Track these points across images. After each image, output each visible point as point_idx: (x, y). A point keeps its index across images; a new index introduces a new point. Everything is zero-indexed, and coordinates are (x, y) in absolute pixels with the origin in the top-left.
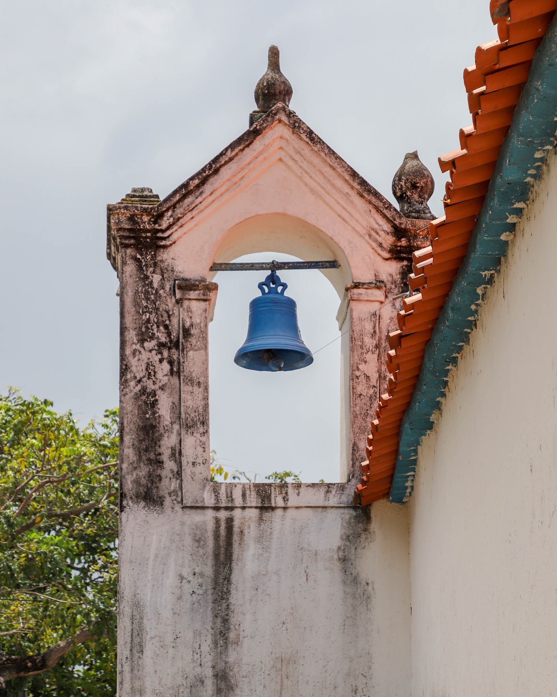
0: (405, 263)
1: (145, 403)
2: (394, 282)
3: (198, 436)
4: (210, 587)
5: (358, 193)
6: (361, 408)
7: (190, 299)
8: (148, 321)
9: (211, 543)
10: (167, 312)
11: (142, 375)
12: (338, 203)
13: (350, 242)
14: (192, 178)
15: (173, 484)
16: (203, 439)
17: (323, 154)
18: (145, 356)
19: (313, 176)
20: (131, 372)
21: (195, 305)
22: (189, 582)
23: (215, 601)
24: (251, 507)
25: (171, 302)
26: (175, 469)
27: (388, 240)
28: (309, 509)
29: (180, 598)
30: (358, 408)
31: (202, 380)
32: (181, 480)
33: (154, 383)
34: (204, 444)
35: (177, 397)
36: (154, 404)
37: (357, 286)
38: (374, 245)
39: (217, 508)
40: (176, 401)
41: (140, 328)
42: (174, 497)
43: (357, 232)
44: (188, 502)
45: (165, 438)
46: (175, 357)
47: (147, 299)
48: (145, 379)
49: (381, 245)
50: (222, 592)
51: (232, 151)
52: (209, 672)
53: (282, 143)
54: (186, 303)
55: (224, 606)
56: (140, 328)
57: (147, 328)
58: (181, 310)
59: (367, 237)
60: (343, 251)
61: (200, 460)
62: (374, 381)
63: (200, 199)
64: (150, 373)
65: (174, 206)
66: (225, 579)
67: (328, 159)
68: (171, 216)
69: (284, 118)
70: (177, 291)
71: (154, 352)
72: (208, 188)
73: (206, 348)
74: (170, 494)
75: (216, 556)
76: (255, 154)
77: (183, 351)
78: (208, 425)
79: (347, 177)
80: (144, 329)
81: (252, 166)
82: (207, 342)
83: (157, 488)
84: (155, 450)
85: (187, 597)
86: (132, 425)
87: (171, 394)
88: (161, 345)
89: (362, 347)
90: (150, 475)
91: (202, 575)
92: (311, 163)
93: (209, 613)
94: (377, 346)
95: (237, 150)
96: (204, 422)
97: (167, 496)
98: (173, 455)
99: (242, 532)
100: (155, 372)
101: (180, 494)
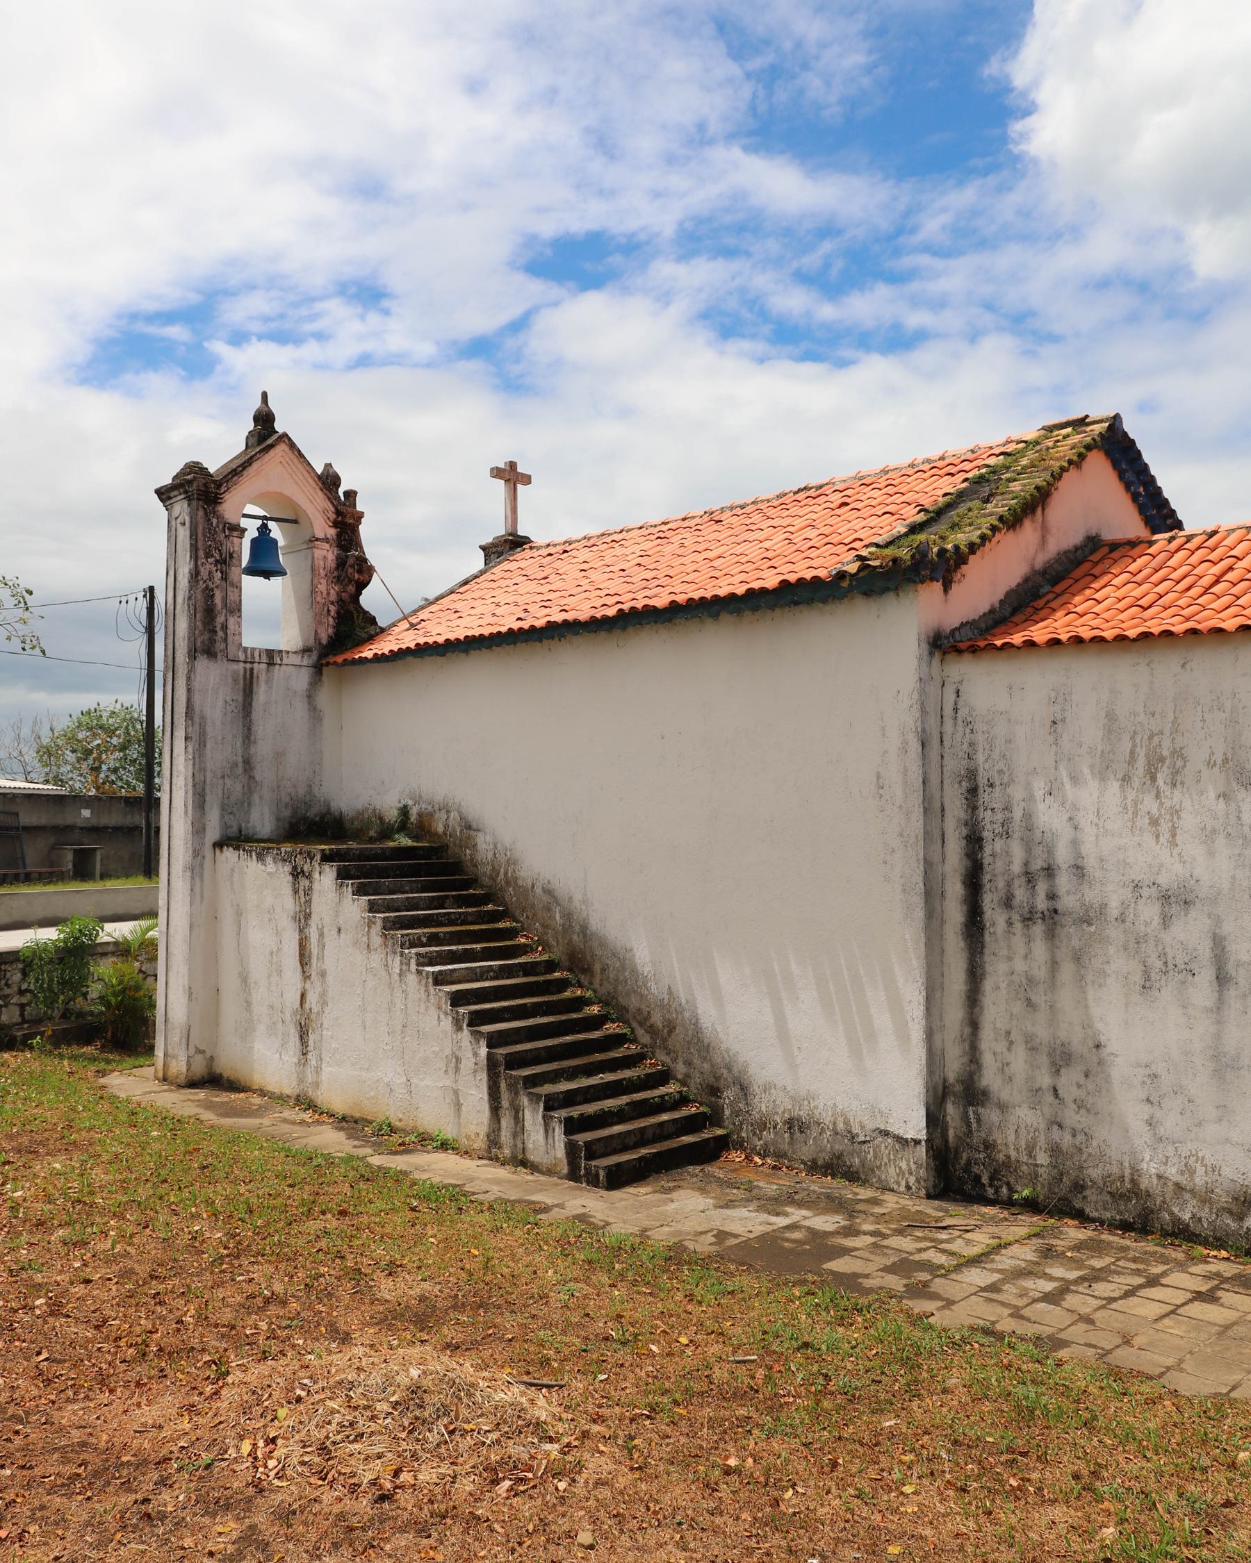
9: (242, 682)
18: (208, 566)
21: (235, 540)
26: (223, 636)
36: (213, 596)
39: (245, 662)
44: (231, 657)
52: (240, 759)
75: (244, 690)
87: (221, 591)
88: (217, 561)
90: (210, 639)
91: (237, 701)
96: (240, 610)
98: (222, 627)
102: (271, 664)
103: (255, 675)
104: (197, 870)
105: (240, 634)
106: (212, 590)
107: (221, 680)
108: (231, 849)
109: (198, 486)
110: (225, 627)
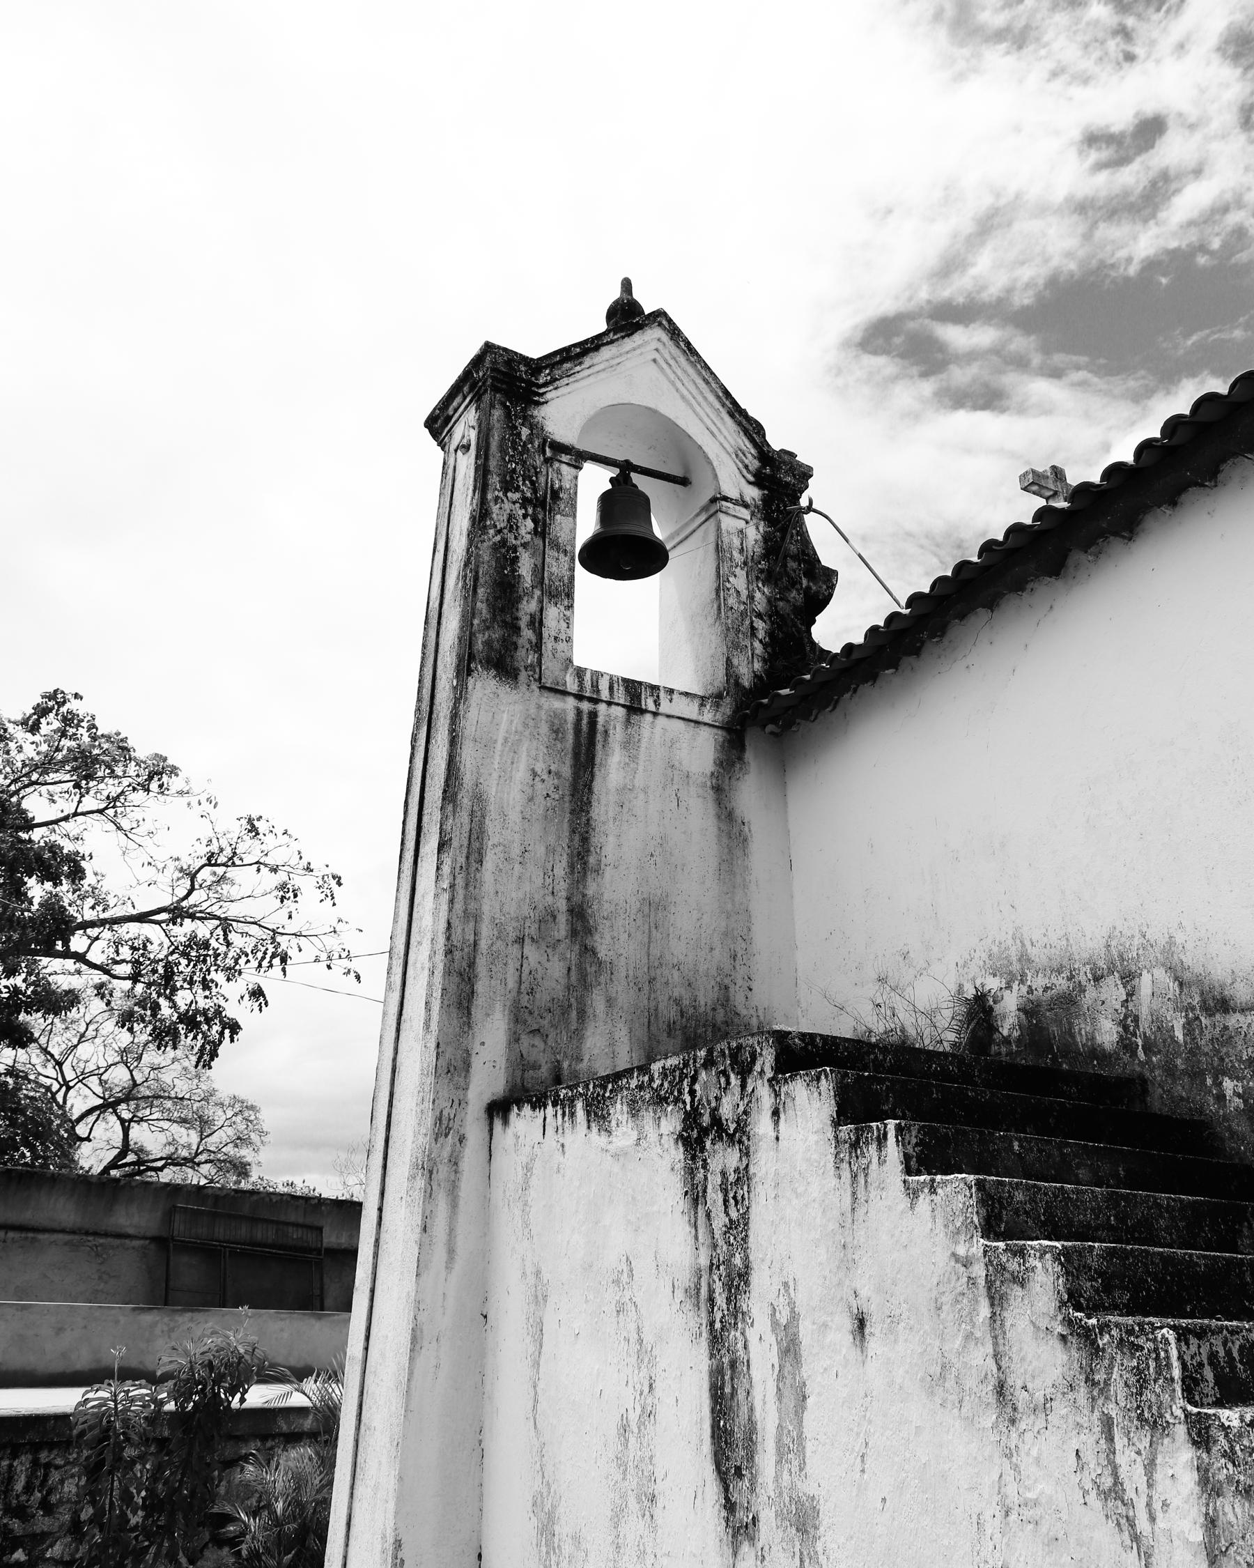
0: (766, 492)
1: (505, 557)
2: (756, 506)
3: (562, 608)
4: (567, 793)
5: (728, 412)
6: (733, 622)
7: (561, 462)
8: (514, 470)
10: (535, 468)
11: (502, 525)
12: (708, 416)
13: (717, 456)
14: (575, 345)
15: (530, 657)
16: (568, 613)
17: (699, 366)
18: (507, 506)
19: (686, 384)
20: (491, 519)
21: (564, 468)
22: (543, 781)
23: (572, 812)
24: (618, 704)
25: (539, 460)
26: (534, 640)
27: (754, 464)
28: (681, 721)
29: (531, 799)
30: (729, 621)
31: (568, 548)
32: (541, 655)
33: (516, 538)
34: (568, 619)
35: (540, 559)
37: (726, 499)
38: (741, 465)
39: (579, 697)
40: (539, 564)
41: (505, 476)
42: (531, 673)
43: (725, 448)
45: (525, 603)
46: (540, 517)
47: (514, 449)
48: (505, 531)
49: (746, 467)
50: (581, 802)
51: (614, 335)
53: (660, 346)
54: (556, 465)
55: (584, 819)
56: (505, 476)
57: (512, 477)
58: (550, 470)
59: (734, 456)
60: (710, 463)
61: (563, 636)
62: (744, 597)
63: (578, 368)
64: (511, 527)
65: (552, 366)
66: (585, 786)
67: (704, 373)
68: (548, 374)
69: (664, 322)
70: (547, 449)
71: (517, 505)
72: (587, 361)
73: (574, 516)
74: (526, 668)
75: (576, 755)
76: (634, 345)
77: (550, 513)
78: (573, 599)
79: (721, 394)
80: (508, 478)
81: (629, 356)
82: (575, 508)
83: (512, 657)
84: (512, 613)
85: (540, 799)
86: (487, 578)
87: (533, 555)
88: (525, 500)
89: (731, 559)
91: (558, 775)
92: (685, 372)
93: (566, 826)
94: (745, 563)
95: (619, 335)
96: (570, 595)
97: (522, 668)
98: (531, 624)
99: (606, 732)
100: (517, 527)
101: (537, 670)
102: (634, 709)
103: (600, 727)
104: (443, 1171)
105: (569, 640)
106: (514, 549)
107: (526, 725)
108: (527, 1109)
109: (494, 362)
110: (537, 623)
